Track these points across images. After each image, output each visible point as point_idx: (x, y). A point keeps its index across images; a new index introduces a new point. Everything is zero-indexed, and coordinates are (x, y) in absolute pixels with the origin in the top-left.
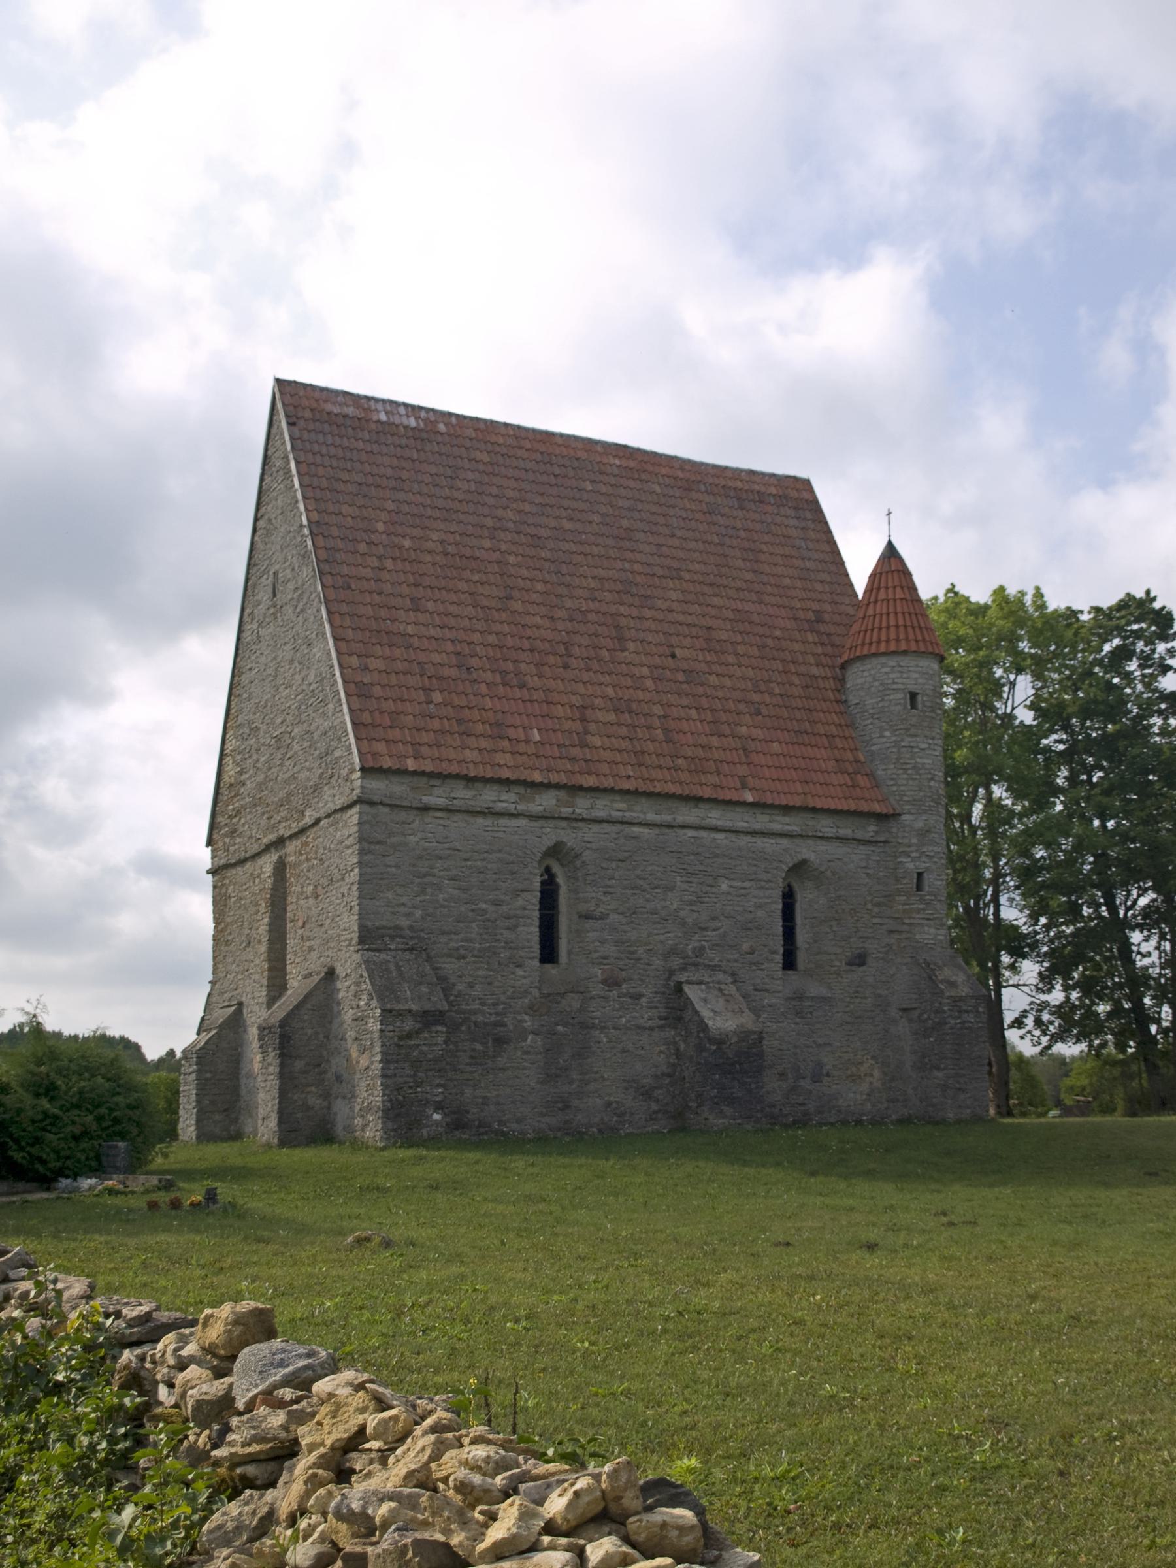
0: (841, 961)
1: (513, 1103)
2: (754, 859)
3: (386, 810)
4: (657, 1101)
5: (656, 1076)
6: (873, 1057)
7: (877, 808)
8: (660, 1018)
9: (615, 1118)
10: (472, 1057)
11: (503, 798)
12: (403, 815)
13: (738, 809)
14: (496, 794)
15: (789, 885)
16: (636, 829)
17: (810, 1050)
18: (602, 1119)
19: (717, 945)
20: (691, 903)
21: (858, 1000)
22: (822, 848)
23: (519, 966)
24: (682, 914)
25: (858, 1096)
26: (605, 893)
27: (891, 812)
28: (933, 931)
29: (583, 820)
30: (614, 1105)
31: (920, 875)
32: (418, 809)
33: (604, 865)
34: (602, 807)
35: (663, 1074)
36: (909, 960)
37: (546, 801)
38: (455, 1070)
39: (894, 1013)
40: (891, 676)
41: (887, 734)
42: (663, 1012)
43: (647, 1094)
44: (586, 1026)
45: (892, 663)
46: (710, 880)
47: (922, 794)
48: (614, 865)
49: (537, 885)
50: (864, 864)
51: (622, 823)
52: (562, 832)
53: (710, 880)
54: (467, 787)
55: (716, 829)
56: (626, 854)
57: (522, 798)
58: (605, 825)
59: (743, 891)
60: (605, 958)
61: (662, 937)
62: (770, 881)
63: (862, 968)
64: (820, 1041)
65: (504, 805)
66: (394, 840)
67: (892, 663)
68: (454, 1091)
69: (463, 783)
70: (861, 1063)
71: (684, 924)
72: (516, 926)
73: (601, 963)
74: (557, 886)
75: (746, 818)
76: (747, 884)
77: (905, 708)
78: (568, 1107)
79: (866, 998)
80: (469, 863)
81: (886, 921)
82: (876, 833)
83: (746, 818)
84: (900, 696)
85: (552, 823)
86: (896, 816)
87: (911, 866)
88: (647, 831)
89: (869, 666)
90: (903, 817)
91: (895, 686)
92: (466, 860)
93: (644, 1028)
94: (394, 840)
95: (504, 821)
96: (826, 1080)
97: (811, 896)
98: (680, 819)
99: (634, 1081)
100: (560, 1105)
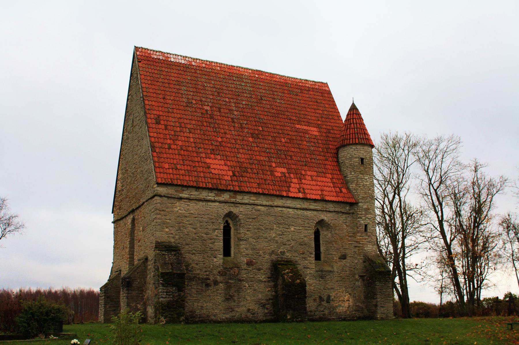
0: (337, 257)
2: (303, 219)
3: (166, 199)
4: (267, 309)
6: (350, 294)
7: (349, 201)
8: (268, 278)
9: (251, 315)
10: (197, 291)
11: (209, 195)
12: (172, 201)
13: (297, 200)
14: (207, 193)
15: (317, 229)
16: (259, 207)
17: (325, 291)
18: (246, 315)
19: (290, 251)
20: (280, 235)
21: (344, 272)
22: (329, 215)
23: (215, 257)
24: (276, 239)
25: (344, 309)
26: (247, 231)
27: (355, 202)
28: (371, 246)
29: (239, 203)
30: (251, 310)
31: (366, 226)
32: (177, 198)
33: (247, 220)
34: (246, 199)
35: (270, 299)
36: (362, 257)
37: (226, 196)
39: (357, 277)
41: (353, 173)
42: (269, 274)
44: (240, 280)
46: (287, 227)
47: (366, 195)
48: (251, 220)
49: (222, 227)
50: (345, 221)
51: (254, 205)
52: (231, 208)
53: (287, 227)
54: (196, 191)
55: (289, 208)
56: (255, 216)
57: (217, 195)
58: (247, 205)
60: (247, 255)
61: (269, 248)
62: (309, 227)
63: (344, 260)
65: (210, 197)
66: (168, 210)
67: (354, 148)
68: (190, 304)
69: (195, 189)
71: (277, 242)
72: (214, 242)
73: (246, 257)
75: (301, 204)
76: (301, 228)
77: (359, 164)
78: (233, 311)
79: (346, 271)
80: (197, 219)
81: (353, 243)
82: (349, 210)
83: (301, 204)
84: (357, 159)
85: (228, 204)
87: (362, 222)
89: (346, 149)
90: (360, 204)
91: (355, 156)
92: (196, 218)
93: (262, 281)
94: (168, 210)
95: (210, 203)
97: (325, 233)
98: (276, 204)
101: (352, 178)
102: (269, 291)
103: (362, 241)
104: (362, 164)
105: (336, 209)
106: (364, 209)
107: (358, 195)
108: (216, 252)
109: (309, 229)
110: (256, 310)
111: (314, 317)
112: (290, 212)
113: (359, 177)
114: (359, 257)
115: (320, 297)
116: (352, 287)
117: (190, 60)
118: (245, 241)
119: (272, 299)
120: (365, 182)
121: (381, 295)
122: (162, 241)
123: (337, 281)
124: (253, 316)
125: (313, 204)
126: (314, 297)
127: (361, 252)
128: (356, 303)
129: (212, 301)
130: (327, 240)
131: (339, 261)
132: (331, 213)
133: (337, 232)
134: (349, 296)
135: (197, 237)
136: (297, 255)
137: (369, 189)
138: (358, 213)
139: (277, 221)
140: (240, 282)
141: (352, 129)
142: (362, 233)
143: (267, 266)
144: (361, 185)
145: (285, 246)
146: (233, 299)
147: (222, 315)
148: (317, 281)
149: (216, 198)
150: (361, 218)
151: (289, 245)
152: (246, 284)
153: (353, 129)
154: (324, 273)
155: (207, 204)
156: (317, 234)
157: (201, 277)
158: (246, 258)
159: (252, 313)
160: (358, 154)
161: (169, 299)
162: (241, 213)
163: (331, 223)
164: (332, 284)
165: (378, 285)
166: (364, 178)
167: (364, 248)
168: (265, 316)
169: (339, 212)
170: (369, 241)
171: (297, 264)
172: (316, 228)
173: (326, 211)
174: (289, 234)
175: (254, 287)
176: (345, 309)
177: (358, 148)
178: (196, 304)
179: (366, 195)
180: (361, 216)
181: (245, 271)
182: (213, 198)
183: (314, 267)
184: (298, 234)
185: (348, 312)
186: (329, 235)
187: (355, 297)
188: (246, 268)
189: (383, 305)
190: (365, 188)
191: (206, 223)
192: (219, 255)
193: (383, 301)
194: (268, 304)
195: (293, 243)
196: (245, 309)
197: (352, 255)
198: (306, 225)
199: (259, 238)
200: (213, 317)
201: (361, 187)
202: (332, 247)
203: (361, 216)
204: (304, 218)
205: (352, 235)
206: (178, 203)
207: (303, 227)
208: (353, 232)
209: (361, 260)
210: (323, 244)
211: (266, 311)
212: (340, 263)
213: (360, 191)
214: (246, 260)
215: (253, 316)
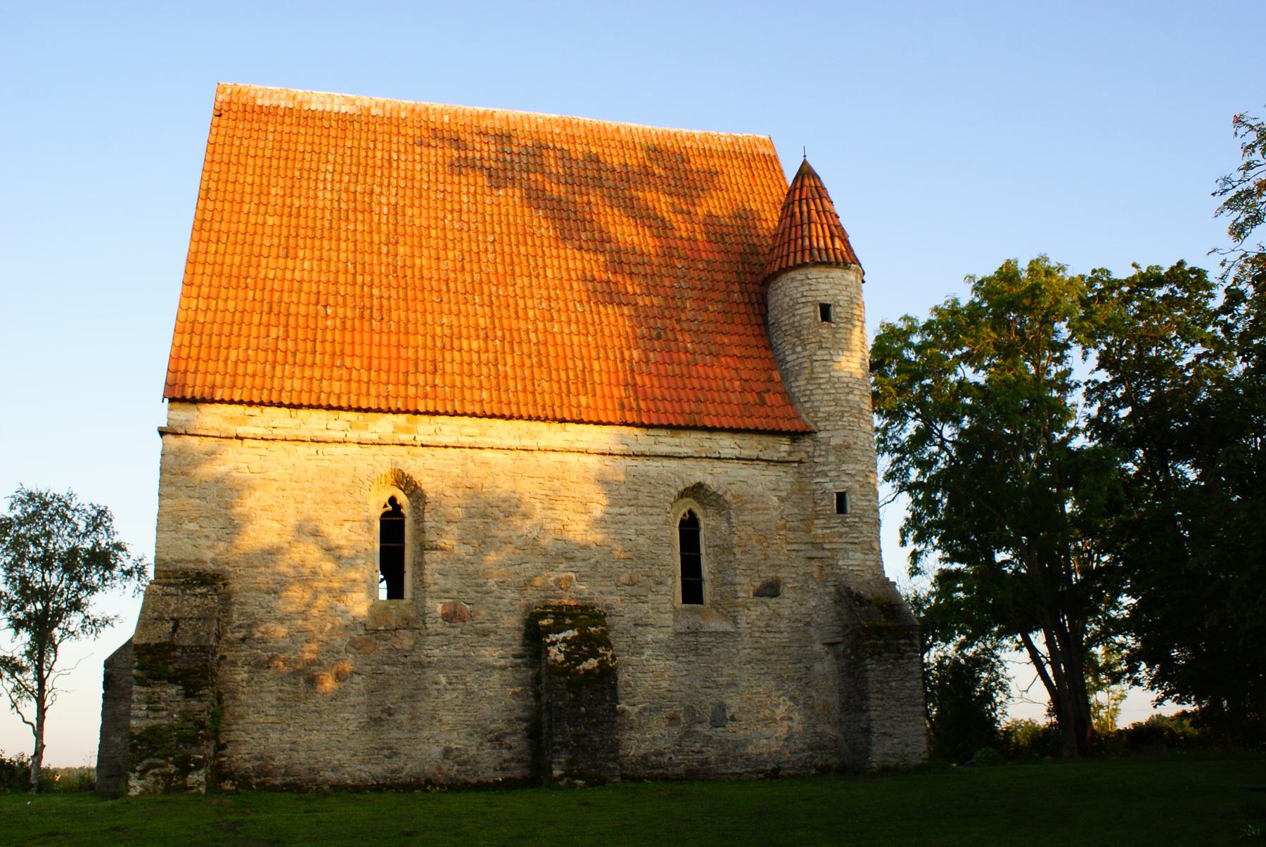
0: (747, 592)
1: (327, 749)
2: (635, 484)
4: (510, 748)
5: (509, 720)
6: (793, 699)
7: (785, 425)
8: (515, 656)
9: (456, 767)
10: (279, 699)
15: (690, 512)
16: (488, 454)
17: (709, 691)
18: (439, 768)
19: (588, 576)
21: (771, 635)
25: (773, 742)
28: (859, 555)
30: (455, 753)
31: (841, 497)
34: (449, 430)
35: (519, 719)
36: (832, 589)
38: (258, 713)
39: (818, 647)
42: (517, 648)
43: (498, 740)
44: (420, 665)
45: (800, 277)
47: (838, 409)
57: (352, 425)
60: (447, 591)
63: (774, 600)
64: (722, 680)
67: (800, 277)
68: (256, 735)
70: (777, 706)
74: (402, 516)
77: (816, 317)
78: (396, 754)
79: (781, 632)
81: (803, 547)
82: (790, 453)
87: (830, 486)
89: (780, 284)
90: (820, 435)
91: (804, 300)
93: (494, 668)
96: (731, 726)
99: (479, 725)
100: (386, 752)
101: (796, 362)
102: (514, 693)
103: (831, 543)
104: (823, 320)
105: (745, 453)
106: (835, 448)
107: (815, 410)
109: (650, 512)
110: (471, 753)
111: (671, 771)
113: (815, 358)
114: (821, 590)
115: (690, 711)
116: (800, 679)
119: (525, 720)
121: (882, 699)
122: (176, 557)
124: (463, 768)
125: (669, 440)
126: (669, 712)
127: (827, 575)
128: (814, 726)
129: (325, 727)
131: (756, 605)
133: (748, 518)
134: (791, 704)
137: (847, 390)
138: (816, 460)
140: (419, 671)
141: (796, 227)
142: (828, 518)
143: (512, 623)
144: (824, 381)
145: (572, 563)
146: (395, 721)
147: (359, 767)
148: (680, 662)
150: (825, 474)
151: (584, 560)
152: (441, 675)
153: (799, 228)
154: (703, 640)
155: (320, 452)
156: (689, 529)
159: (458, 759)
160: (813, 293)
161: (155, 722)
163: (725, 493)
164: (731, 672)
165: (873, 670)
166: (832, 360)
167: (838, 561)
168: (503, 769)
169: (752, 460)
170: (852, 540)
171: (611, 616)
172: (685, 510)
173: (707, 457)
177: (810, 276)
179: (838, 409)
180: (825, 468)
183: (670, 623)
184: (616, 526)
186: (724, 526)
187: (813, 708)
188: (442, 630)
189: (890, 730)
190: (836, 388)
193: (891, 717)
194: (515, 733)
196: (436, 751)
197: (799, 585)
198: (640, 502)
200: (331, 774)
201: (823, 386)
202: (731, 562)
203: (825, 468)
204: (635, 480)
205: (796, 524)
207: (632, 508)
208: (800, 517)
209: (827, 598)
210: (707, 554)
211: (506, 754)
212: (759, 609)
215: (463, 768)
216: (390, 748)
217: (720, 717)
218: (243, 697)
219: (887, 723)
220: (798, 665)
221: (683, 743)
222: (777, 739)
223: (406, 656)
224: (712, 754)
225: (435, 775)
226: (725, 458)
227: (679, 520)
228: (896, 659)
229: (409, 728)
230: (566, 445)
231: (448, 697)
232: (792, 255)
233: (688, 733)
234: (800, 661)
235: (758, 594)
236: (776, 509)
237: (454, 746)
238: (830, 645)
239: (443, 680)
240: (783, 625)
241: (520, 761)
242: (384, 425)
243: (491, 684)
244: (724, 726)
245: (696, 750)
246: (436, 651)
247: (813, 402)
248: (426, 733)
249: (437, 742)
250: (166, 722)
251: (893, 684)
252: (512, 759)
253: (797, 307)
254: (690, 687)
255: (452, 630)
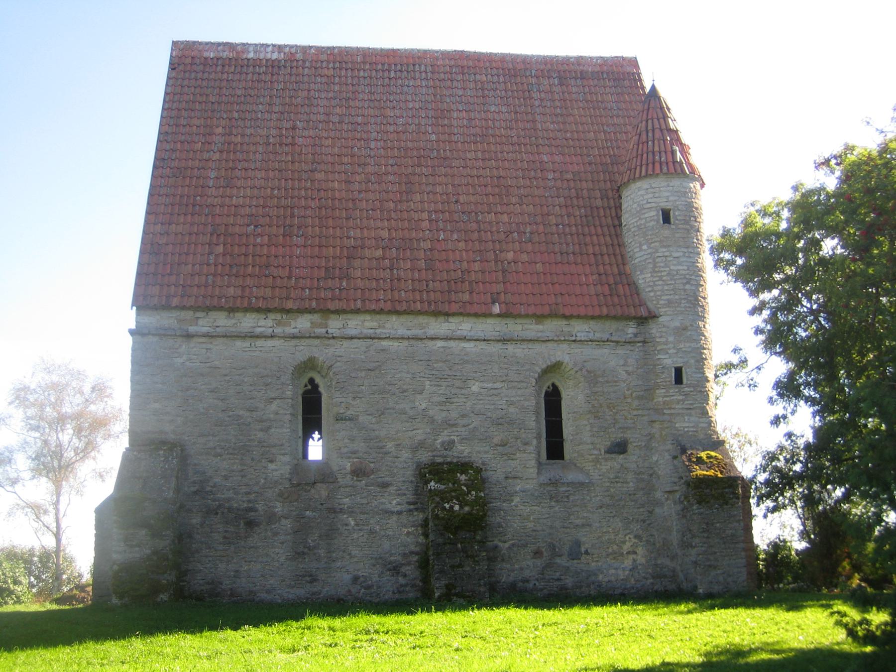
1: (262, 576)
4: (405, 576)
5: (405, 554)
6: (635, 537)
8: (409, 503)
9: (363, 591)
10: (225, 537)
16: (385, 343)
18: (350, 591)
19: (466, 439)
20: (440, 403)
21: (619, 485)
22: (576, 351)
23: (271, 461)
24: (431, 413)
25: (620, 572)
29: (334, 338)
30: (362, 579)
31: (679, 372)
35: (412, 553)
36: (670, 447)
38: (210, 548)
40: (646, 197)
42: (411, 497)
43: (395, 570)
44: (333, 511)
45: (646, 186)
46: (458, 383)
47: (677, 297)
48: (363, 374)
54: (228, 317)
55: (464, 339)
57: (279, 323)
59: (495, 392)
60: (354, 452)
64: (578, 522)
69: (226, 313)
70: (624, 542)
71: (432, 421)
72: (269, 428)
73: (349, 458)
76: (498, 385)
77: (658, 222)
79: (627, 483)
80: (227, 378)
82: (636, 335)
84: (653, 213)
86: (653, 317)
88: (396, 344)
89: (629, 192)
90: (660, 319)
91: (649, 206)
92: (226, 375)
93: (392, 513)
95: (260, 343)
97: (572, 394)
98: (431, 332)
99: (380, 558)
100: (308, 579)
102: (408, 533)
103: (670, 408)
104: (664, 223)
105: (598, 336)
108: (274, 450)
110: (374, 580)
112: (468, 350)
115: (552, 547)
116: (644, 521)
117: (293, 51)
118: (348, 423)
119: (417, 554)
120: (674, 265)
121: (708, 537)
123: (601, 507)
124: (368, 591)
128: (655, 559)
130: (576, 410)
131: (606, 460)
132: (584, 346)
134: (636, 541)
135: (227, 419)
136: (487, 448)
137: (685, 281)
139: (433, 372)
145: (454, 429)
147: (287, 590)
148: (543, 507)
149: (278, 330)
151: (464, 426)
152: (350, 519)
153: (645, 144)
155: (253, 344)
157: (235, 505)
158: (351, 460)
162: (339, 359)
164: (585, 515)
168: (399, 592)
174: (465, 400)
175: (367, 525)
176: (622, 575)
177: (653, 186)
178: (222, 566)
179: (677, 297)
181: (348, 489)
182: (271, 330)
183: (535, 475)
184: (490, 398)
185: (633, 580)
187: (654, 544)
190: (675, 280)
191: (251, 385)
192: (281, 457)
194: (409, 564)
195: (476, 422)
196: (347, 578)
199: (383, 414)
200: (266, 595)
203: (665, 347)
206: (184, 347)
209: (666, 454)
211: (402, 580)
212: (609, 463)
213: (659, 288)
214: (349, 464)
215: (368, 591)
216: (311, 576)
217: (576, 552)
218: (198, 536)
219: (712, 558)
220: (641, 510)
221: (545, 572)
222: (624, 569)
223: (322, 504)
224: (569, 581)
225: (347, 596)
226: (580, 341)
227: (544, 392)
228: (721, 506)
229: (325, 560)
230: (449, 333)
231: (355, 536)
232: (638, 168)
233: (549, 566)
234: (643, 506)
235: (610, 451)
236: (624, 382)
237: (360, 573)
238: (669, 492)
239: (352, 523)
240: (630, 477)
241: (413, 586)
242: (303, 323)
243: (388, 526)
244: (580, 559)
245: (555, 577)
246: (347, 500)
247: (656, 291)
248: (339, 564)
249: (347, 571)
250: (138, 556)
251: (718, 525)
252: (406, 585)
253: (643, 212)
254: (551, 527)
255: (358, 483)
